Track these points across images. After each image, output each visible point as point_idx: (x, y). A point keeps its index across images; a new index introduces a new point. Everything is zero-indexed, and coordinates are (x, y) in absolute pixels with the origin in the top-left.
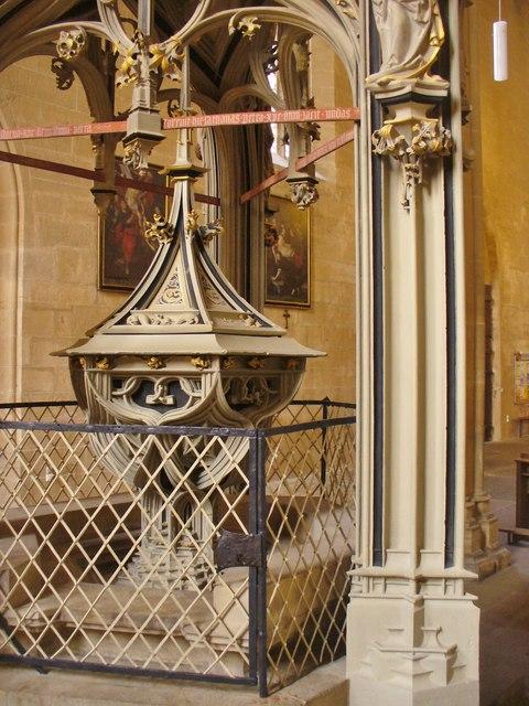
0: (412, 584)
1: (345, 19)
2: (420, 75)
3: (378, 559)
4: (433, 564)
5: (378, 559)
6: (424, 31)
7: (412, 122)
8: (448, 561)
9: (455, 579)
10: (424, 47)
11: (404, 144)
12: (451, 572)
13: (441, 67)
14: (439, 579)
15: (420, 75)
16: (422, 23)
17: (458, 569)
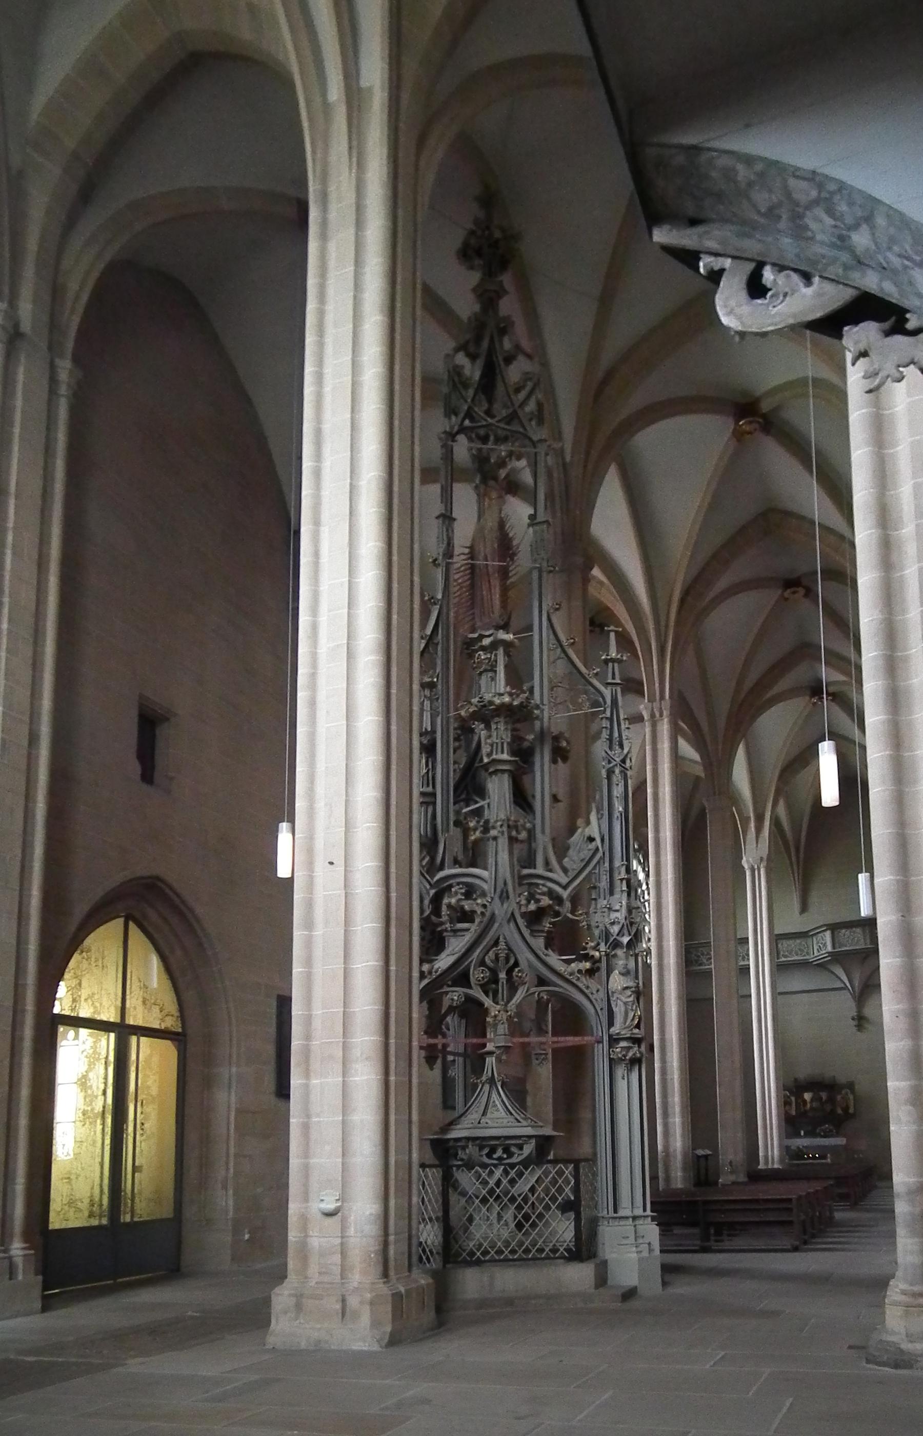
0: (631, 1219)
1: (594, 1001)
2: (632, 1030)
3: (615, 1211)
4: (639, 1212)
5: (615, 1211)
6: (633, 1014)
7: (629, 1048)
8: (645, 1210)
9: (647, 1216)
10: (633, 1019)
11: (625, 1056)
12: (646, 1214)
13: (638, 1026)
14: (641, 1217)
15: (632, 1030)
16: (632, 1010)
17: (648, 1212)
